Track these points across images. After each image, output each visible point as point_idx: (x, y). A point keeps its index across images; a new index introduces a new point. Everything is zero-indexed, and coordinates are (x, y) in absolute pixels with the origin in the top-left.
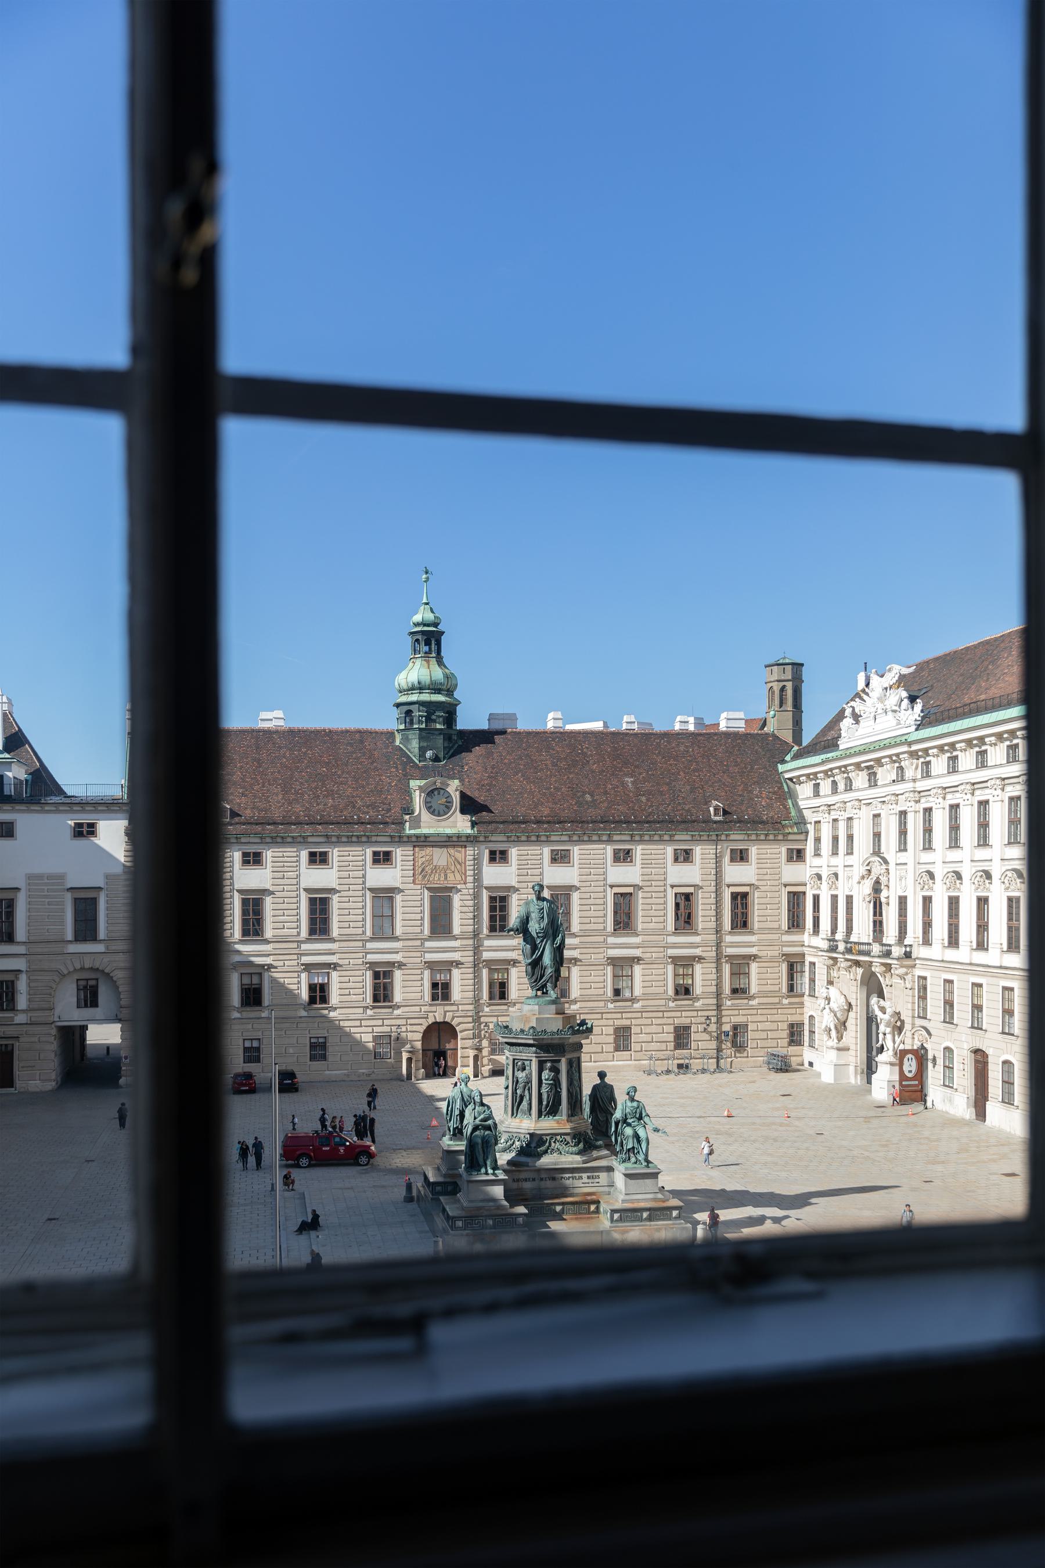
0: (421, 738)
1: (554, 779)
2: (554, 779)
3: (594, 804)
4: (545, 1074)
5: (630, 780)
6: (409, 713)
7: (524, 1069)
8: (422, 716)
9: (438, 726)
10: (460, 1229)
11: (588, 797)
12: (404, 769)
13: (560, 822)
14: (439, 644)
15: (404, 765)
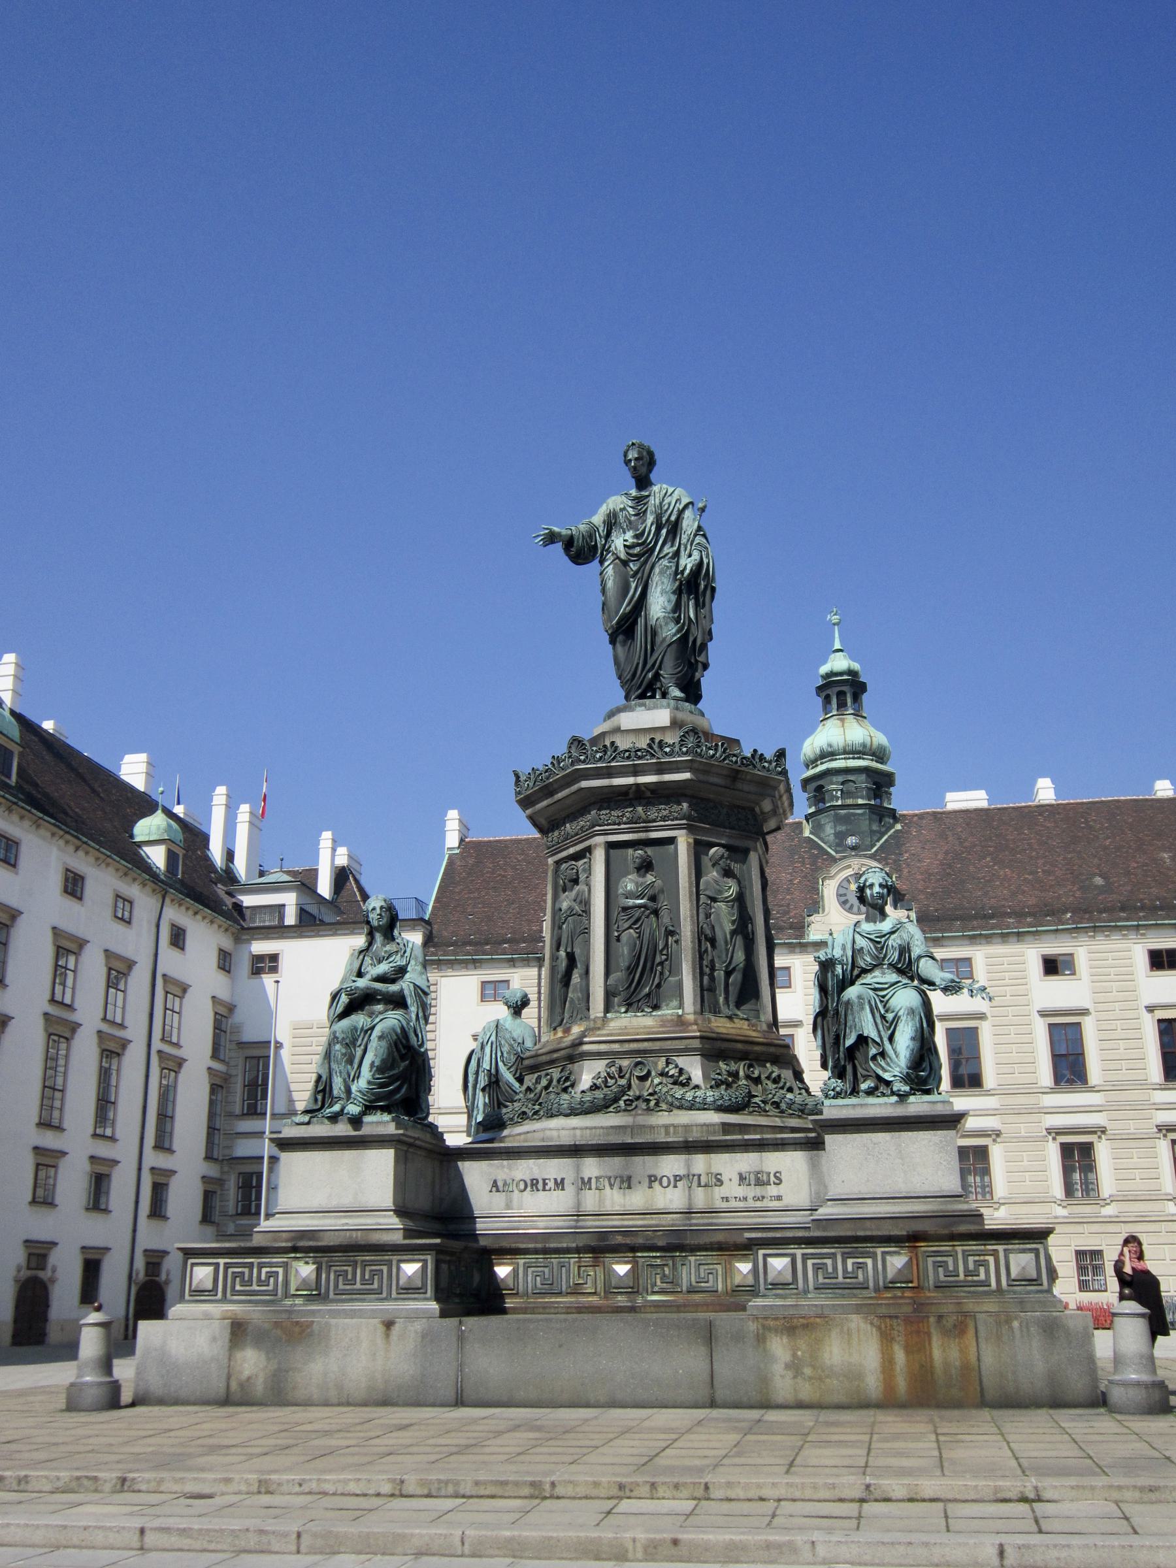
0: (838, 820)
1: (1041, 862)
2: (1041, 862)
3: (1108, 888)
4: (629, 883)
5: (1166, 856)
6: (820, 789)
7: (576, 881)
8: (837, 790)
9: (860, 801)
10: (199, 1294)
11: (1098, 881)
12: (814, 863)
13: (1052, 913)
14: (856, 698)
15: (814, 858)
